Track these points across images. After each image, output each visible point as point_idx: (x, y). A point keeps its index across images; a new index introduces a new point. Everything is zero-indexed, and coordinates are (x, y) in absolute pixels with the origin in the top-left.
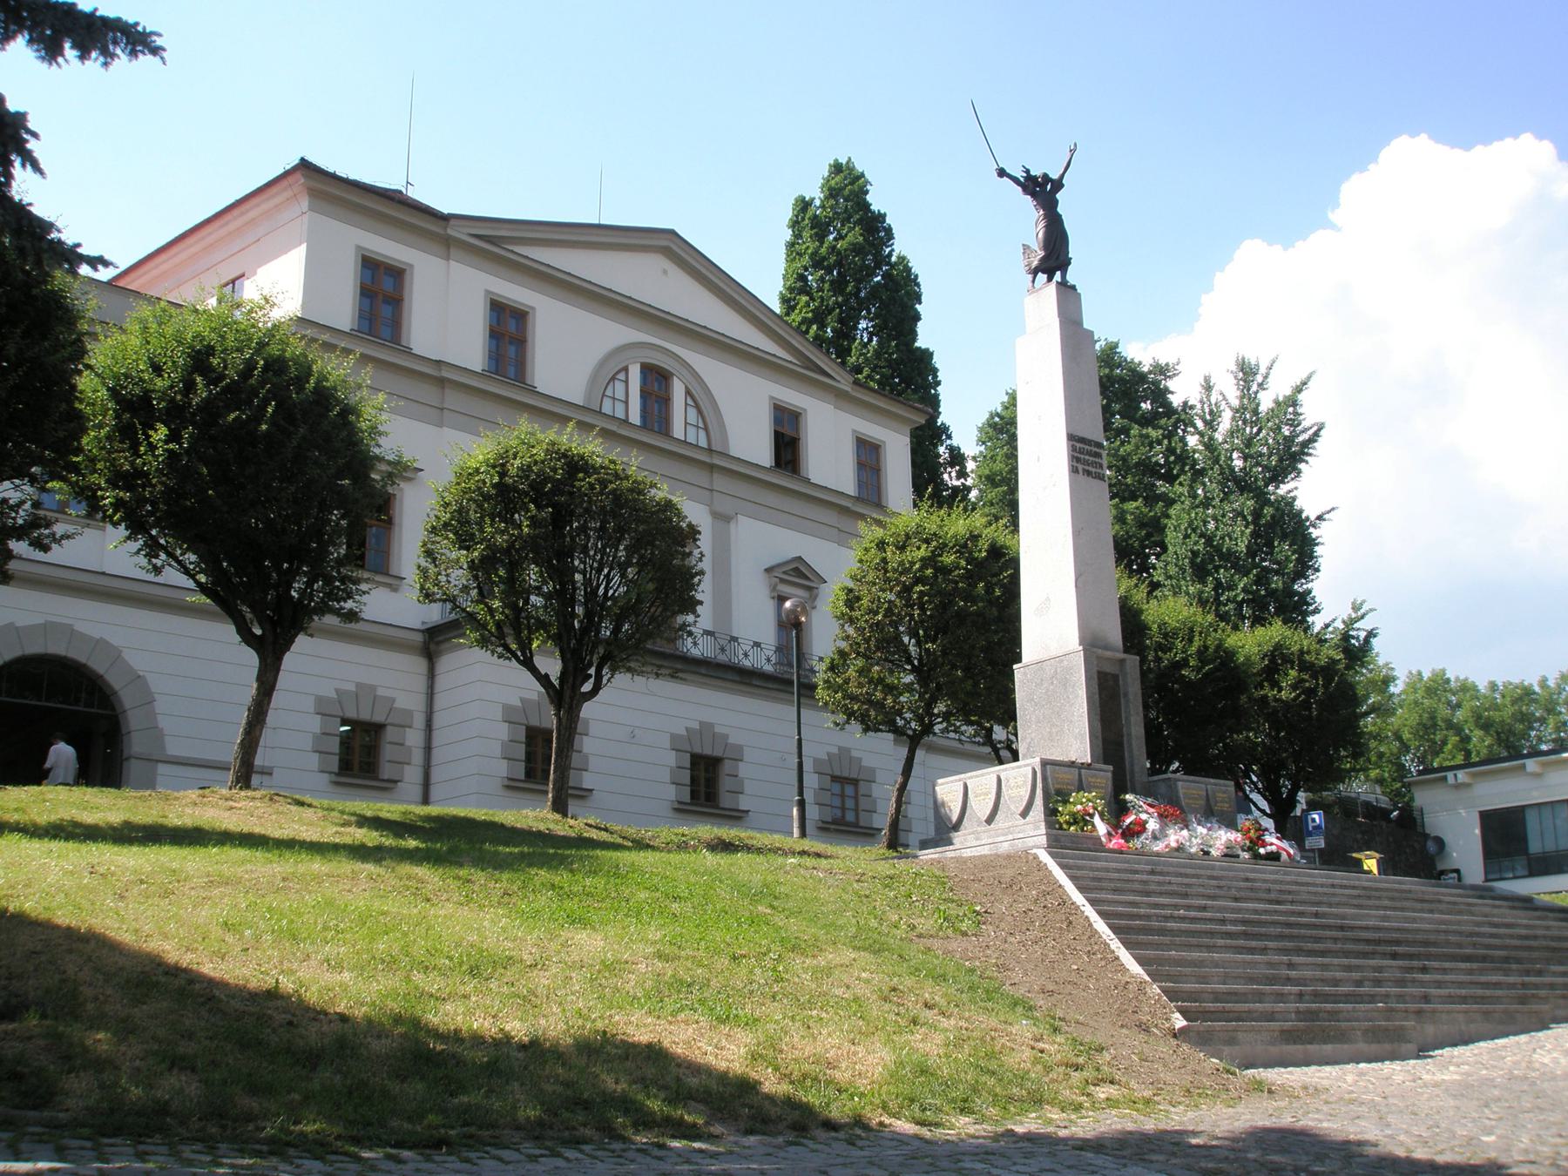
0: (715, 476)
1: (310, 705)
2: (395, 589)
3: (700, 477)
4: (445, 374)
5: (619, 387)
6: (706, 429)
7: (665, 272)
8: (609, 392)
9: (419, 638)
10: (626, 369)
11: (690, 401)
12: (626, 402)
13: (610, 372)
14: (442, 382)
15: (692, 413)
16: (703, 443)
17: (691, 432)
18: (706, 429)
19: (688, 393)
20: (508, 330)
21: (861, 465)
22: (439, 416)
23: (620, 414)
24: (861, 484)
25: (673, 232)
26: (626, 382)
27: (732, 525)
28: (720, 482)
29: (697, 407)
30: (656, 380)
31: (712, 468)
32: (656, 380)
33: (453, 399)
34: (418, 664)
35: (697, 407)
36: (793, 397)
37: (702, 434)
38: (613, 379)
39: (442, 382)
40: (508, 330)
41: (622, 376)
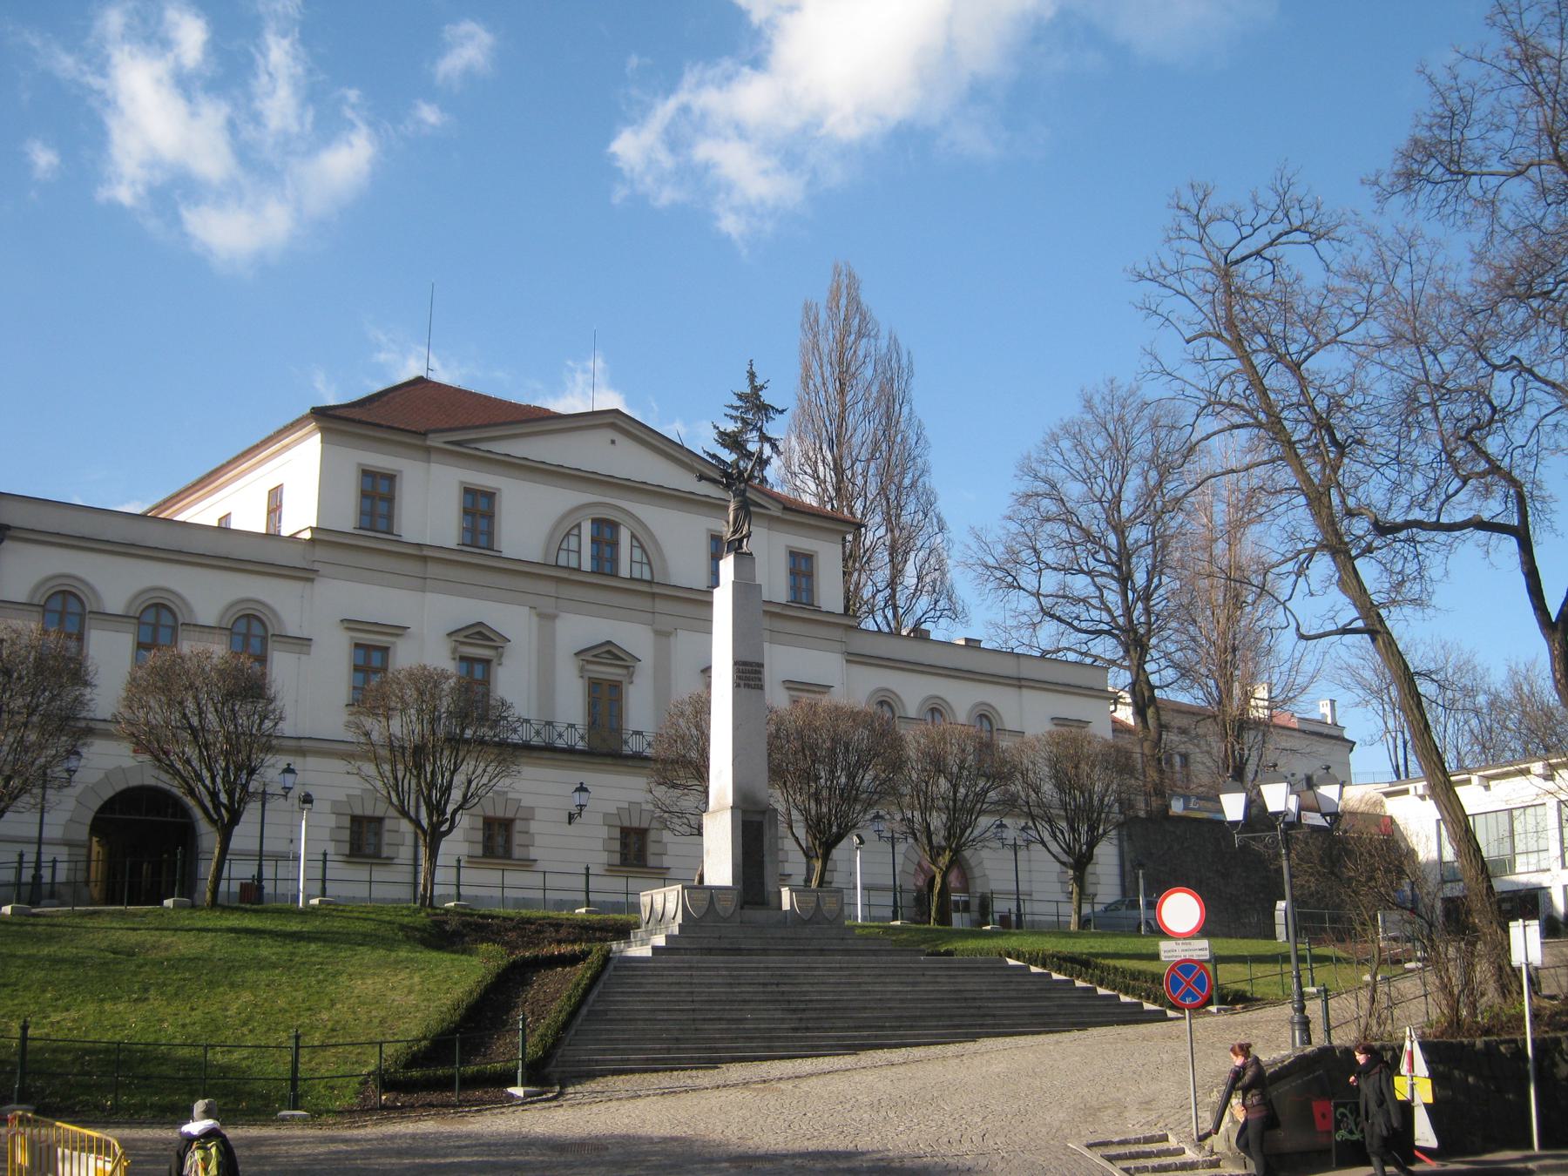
0: (657, 601)
3: (645, 603)
5: (573, 541)
7: (613, 442)
8: (564, 546)
10: (579, 526)
12: (579, 552)
13: (566, 531)
14: (425, 559)
15: (637, 554)
16: (647, 576)
17: (636, 567)
18: (649, 564)
19: (633, 536)
20: (479, 510)
21: (794, 573)
22: (423, 584)
23: (574, 564)
24: (795, 588)
26: (579, 536)
27: (672, 638)
28: (660, 605)
29: (642, 547)
30: (605, 533)
31: (653, 595)
32: (605, 533)
33: (433, 570)
35: (642, 547)
37: (646, 568)
38: (568, 534)
39: (425, 559)
40: (479, 510)
41: (575, 532)
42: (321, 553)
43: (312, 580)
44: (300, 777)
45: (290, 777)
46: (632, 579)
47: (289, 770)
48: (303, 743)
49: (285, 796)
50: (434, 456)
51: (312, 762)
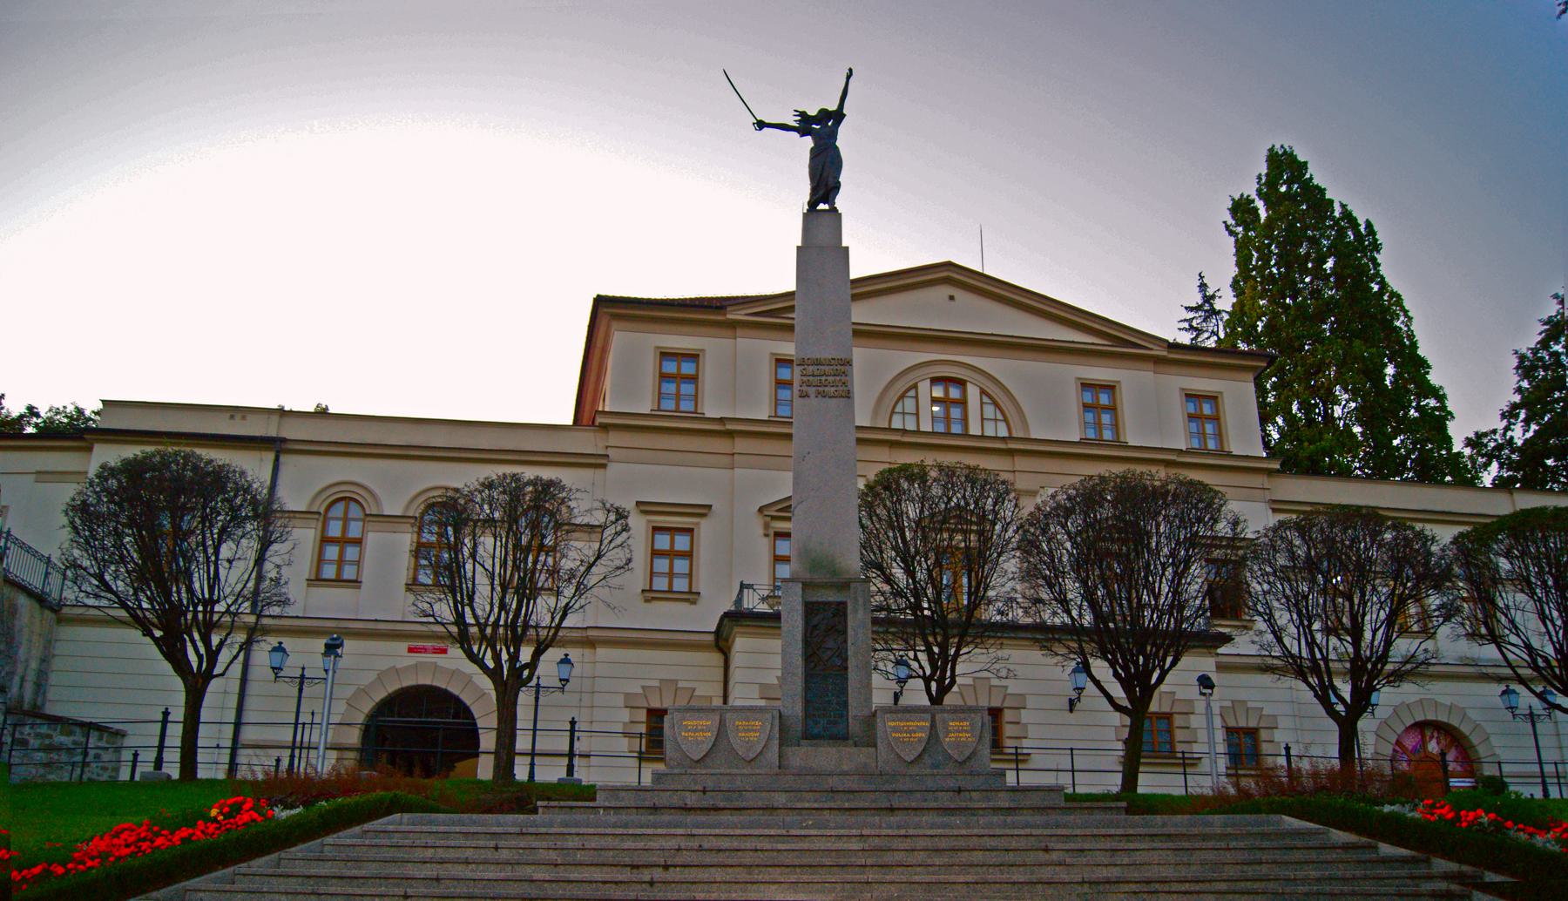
1: (620, 701)
2: (694, 603)
4: (729, 427)
5: (909, 404)
6: (1005, 420)
7: (952, 298)
8: (899, 409)
9: (711, 638)
10: (915, 387)
11: (986, 399)
12: (917, 414)
14: (730, 434)
15: (990, 411)
16: (1003, 432)
19: (983, 392)
25: (949, 265)
26: (916, 397)
33: (741, 445)
34: (716, 658)
36: (1099, 373)
38: (902, 397)
41: (912, 393)
42: (614, 438)
43: (604, 466)
44: (577, 671)
45: (566, 667)
46: (983, 437)
47: (566, 660)
48: (590, 633)
49: (562, 689)
50: (739, 332)
51: (602, 652)
